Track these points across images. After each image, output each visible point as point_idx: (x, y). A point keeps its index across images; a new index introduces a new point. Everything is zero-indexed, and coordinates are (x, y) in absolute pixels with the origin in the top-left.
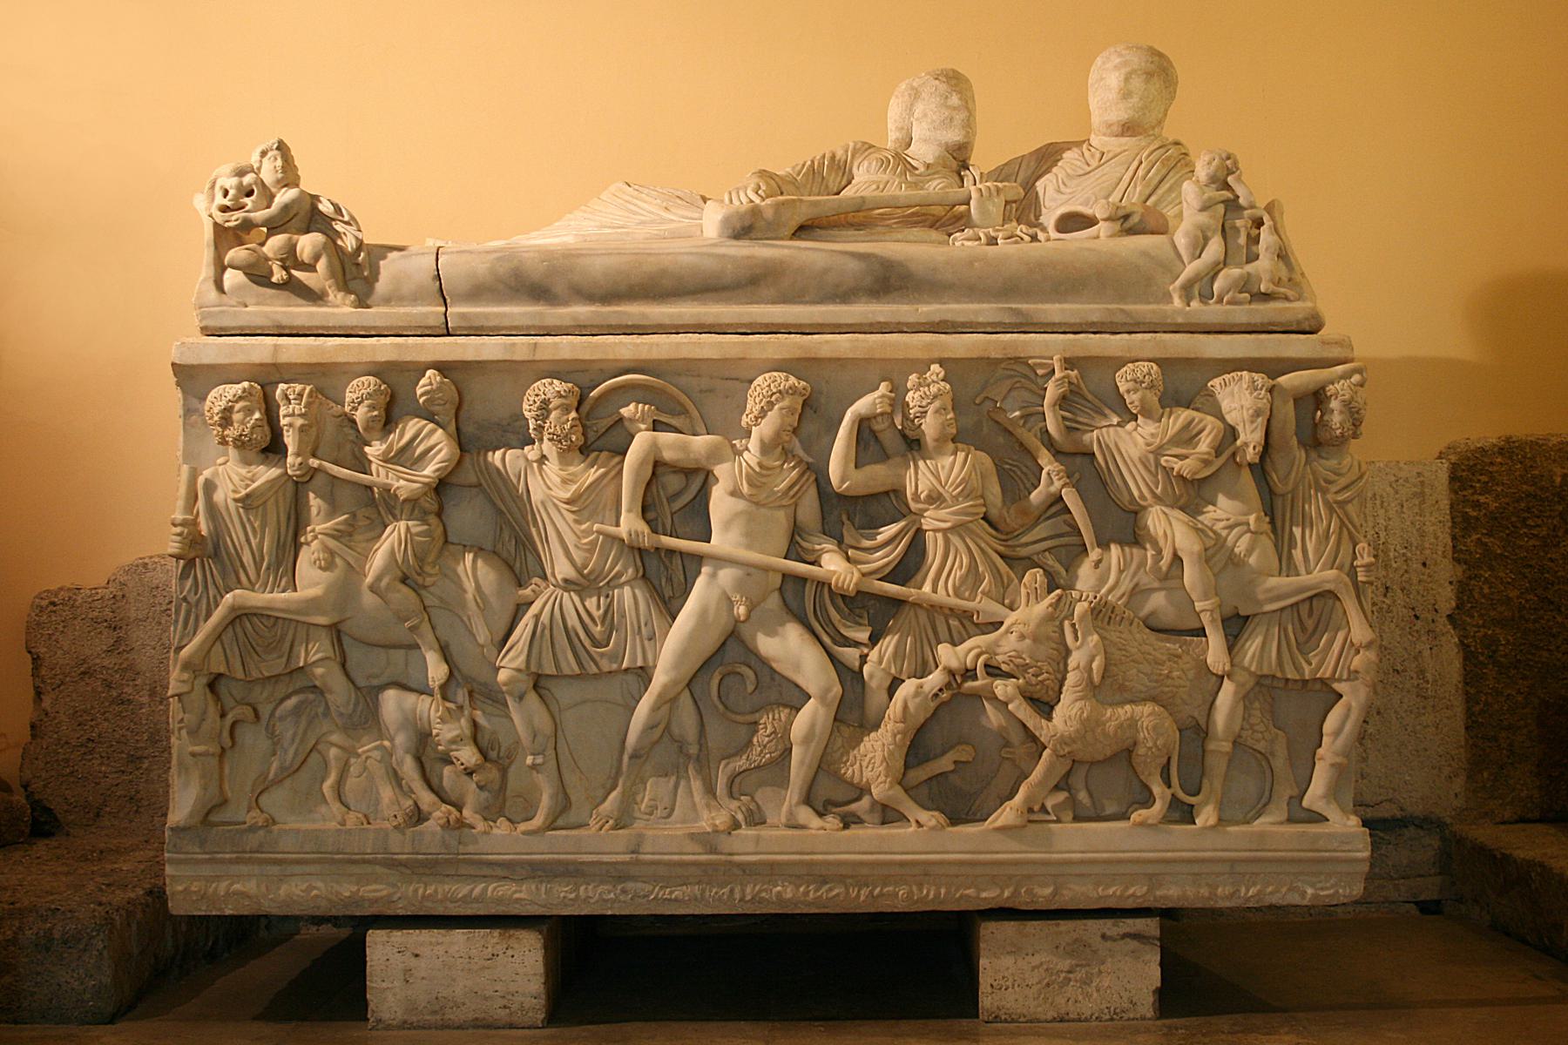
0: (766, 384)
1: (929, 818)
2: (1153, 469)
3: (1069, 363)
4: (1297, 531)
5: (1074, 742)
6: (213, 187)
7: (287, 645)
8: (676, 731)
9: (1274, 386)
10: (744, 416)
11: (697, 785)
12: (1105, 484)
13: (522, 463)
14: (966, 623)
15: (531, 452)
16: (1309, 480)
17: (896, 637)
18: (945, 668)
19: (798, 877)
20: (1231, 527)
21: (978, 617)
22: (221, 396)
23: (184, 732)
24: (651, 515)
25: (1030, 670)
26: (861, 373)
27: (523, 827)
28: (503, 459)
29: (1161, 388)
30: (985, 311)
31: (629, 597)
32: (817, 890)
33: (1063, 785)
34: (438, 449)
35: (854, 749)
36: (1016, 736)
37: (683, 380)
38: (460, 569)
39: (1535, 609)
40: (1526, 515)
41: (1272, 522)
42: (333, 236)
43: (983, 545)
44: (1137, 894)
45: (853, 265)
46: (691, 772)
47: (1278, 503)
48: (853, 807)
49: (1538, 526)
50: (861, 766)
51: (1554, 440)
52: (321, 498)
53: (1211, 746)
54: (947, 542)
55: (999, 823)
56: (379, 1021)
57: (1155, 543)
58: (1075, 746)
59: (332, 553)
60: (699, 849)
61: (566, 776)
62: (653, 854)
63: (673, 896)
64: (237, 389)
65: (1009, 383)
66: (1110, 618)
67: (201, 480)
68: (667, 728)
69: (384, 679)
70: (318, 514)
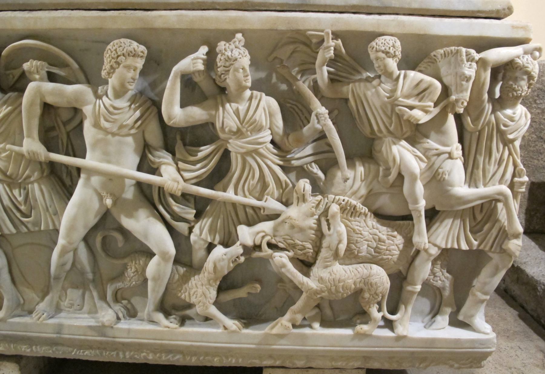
0: (114, 48)
1: (232, 324)
2: (389, 113)
4: (481, 159)
5: (323, 292)
9: (480, 59)
10: (103, 71)
11: (95, 294)
16: (493, 124)
17: (210, 220)
18: (240, 245)
20: (439, 155)
21: (264, 212)
25: (298, 247)
29: (400, 56)
32: (166, 356)
35: (185, 284)
39: (535, 141)
40: (536, 98)
43: (269, 163)
46: (92, 288)
49: (541, 103)
50: (189, 294)
54: (244, 162)
55: (275, 331)
57: (386, 162)
58: (323, 294)
62: (69, 335)
63: (85, 354)
65: (291, 47)
66: (352, 213)
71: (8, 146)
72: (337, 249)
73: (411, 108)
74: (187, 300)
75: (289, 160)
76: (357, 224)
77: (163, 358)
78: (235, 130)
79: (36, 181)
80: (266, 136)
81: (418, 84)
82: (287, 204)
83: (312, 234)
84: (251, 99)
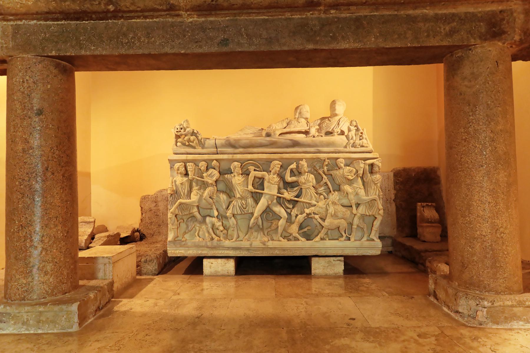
1: (303, 239)
3: (328, 159)
6: (175, 128)
7: (189, 209)
8: (258, 224)
11: (262, 233)
12: (334, 180)
13: (231, 177)
14: (310, 205)
15: (232, 175)
19: (279, 249)
20: (357, 188)
22: (177, 165)
23: (171, 224)
24: (253, 186)
26: (290, 161)
27: (231, 241)
28: (227, 176)
30: (312, 149)
31: (250, 201)
33: (327, 234)
34: (216, 174)
36: (318, 225)
37: (259, 162)
38: (220, 195)
41: (364, 187)
42: (197, 137)
44: (340, 253)
45: (289, 142)
47: (365, 183)
48: (290, 237)
51: (413, 168)
53: (353, 227)
54: (306, 190)
56: (205, 275)
59: (197, 193)
60: (262, 245)
61: (239, 232)
64: (180, 164)
65: (317, 162)
67: (174, 180)
68: (256, 223)
69: (206, 214)
71: (244, 188)
72: (332, 214)
73: (348, 176)
74: (290, 232)
75: (317, 191)
76: (336, 207)
77: (282, 253)
78: (304, 182)
80: (311, 184)
81: (349, 170)
82: (318, 202)
83: (324, 209)
84: (307, 175)
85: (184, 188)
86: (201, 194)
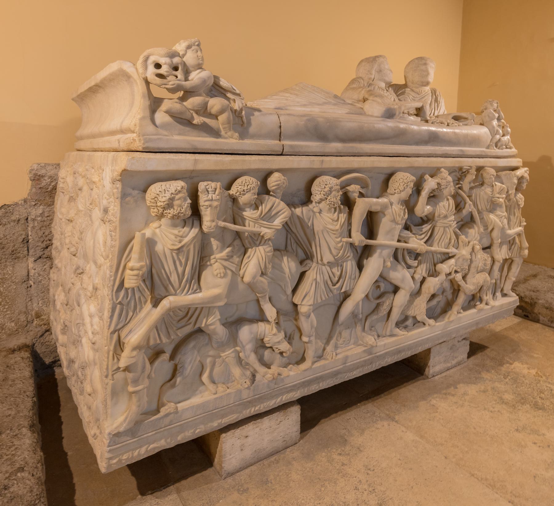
52: (217, 240)
59: (225, 268)
70: (217, 249)
79: (350, 260)
85: (183, 261)
86: (234, 269)
